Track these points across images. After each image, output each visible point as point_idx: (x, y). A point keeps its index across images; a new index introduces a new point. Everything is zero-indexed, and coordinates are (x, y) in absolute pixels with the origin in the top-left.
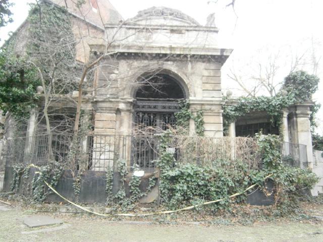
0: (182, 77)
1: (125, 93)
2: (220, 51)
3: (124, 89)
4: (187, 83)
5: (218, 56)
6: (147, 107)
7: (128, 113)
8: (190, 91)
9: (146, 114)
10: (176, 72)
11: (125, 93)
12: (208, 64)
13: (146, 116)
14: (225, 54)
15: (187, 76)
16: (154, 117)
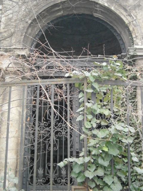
0: (117, 12)
1: (13, 41)
3: (11, 35)
4: (127, 22)
8: (134, 36)
10: (106, 5)
11: (13, 41)
15: (126, 10)
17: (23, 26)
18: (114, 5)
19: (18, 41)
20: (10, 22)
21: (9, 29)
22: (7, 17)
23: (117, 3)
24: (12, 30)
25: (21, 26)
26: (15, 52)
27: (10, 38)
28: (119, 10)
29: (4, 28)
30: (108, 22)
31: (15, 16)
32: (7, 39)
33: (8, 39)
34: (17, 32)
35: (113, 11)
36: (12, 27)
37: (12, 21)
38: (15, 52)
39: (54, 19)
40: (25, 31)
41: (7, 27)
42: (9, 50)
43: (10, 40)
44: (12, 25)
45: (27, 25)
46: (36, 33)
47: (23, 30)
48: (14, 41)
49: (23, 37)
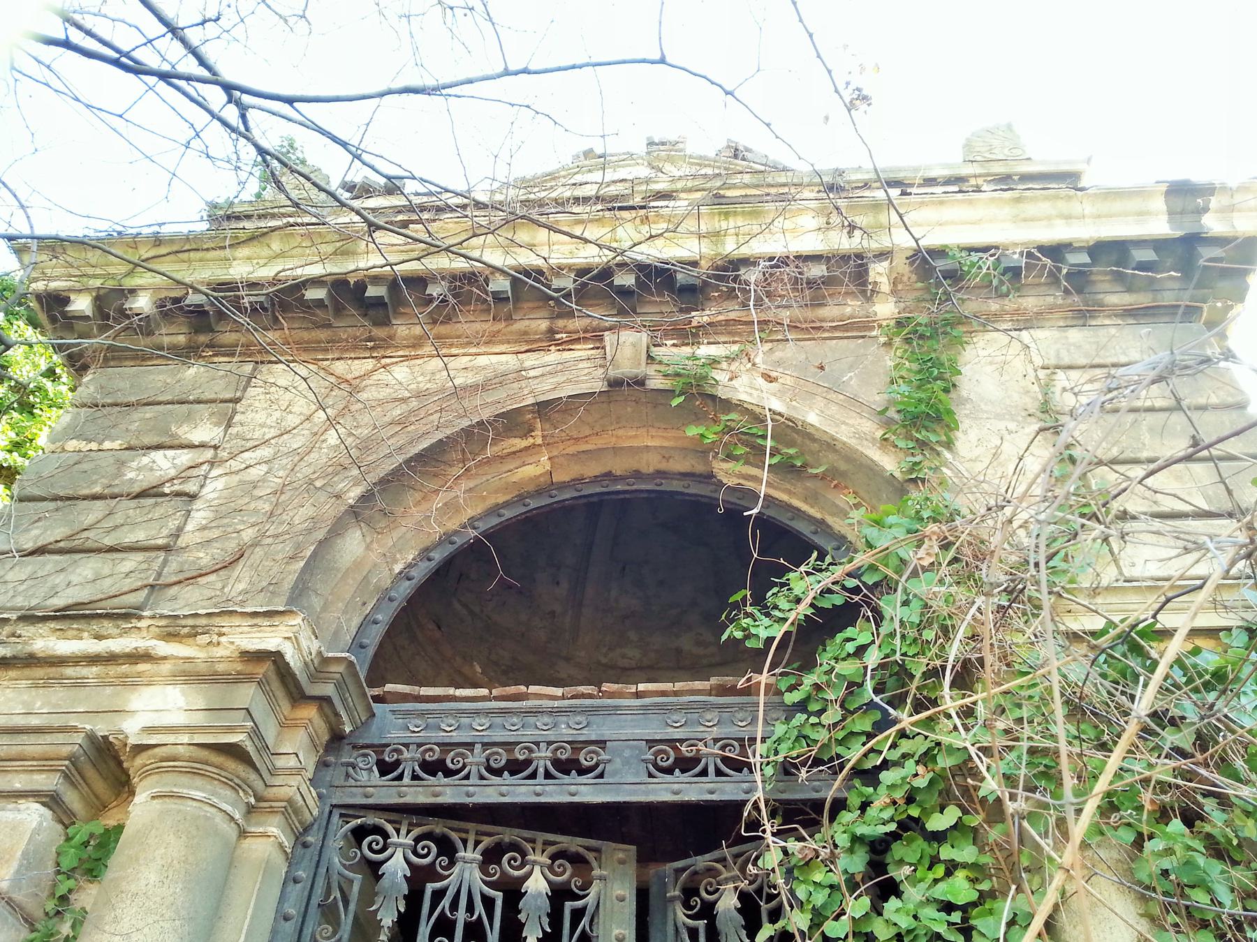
2: (1159, 204)
5: (1159, 244)
6: (477, 757)
7: (213, 800)
9: (470, 855)
12: (1075, 335)
13: (468, 873)
14: (1213, 224)
16: (559, 895)
17: (308, 511)
18: (819, 401)
19: (264, 584)
20: (247, 500)
21: (230, 530)
22: (236, 478)
23: (833, 396)
24: (248, 535)
25: (301, 515)
26: (220, 635)
27: (221, 573)
28: (847, 424)
29: (204, 528)
30: (797, 503)
31: (281, 473)
32: (202, 580)
33: (212, 577)
34: (270, 540)
35: (817, 429)
36: (252, 520)
37: (258, 493)
38: (223, 639)
39: (501, 499)
40: (320, 535)
41: (226, 521)
42: (190, 622)
43: (219, 585)
44: (256, 511)
45: (331, 510)
46: (398, 568)
47: (309, 531)
48: (241, 586)
49: (302, 564)
